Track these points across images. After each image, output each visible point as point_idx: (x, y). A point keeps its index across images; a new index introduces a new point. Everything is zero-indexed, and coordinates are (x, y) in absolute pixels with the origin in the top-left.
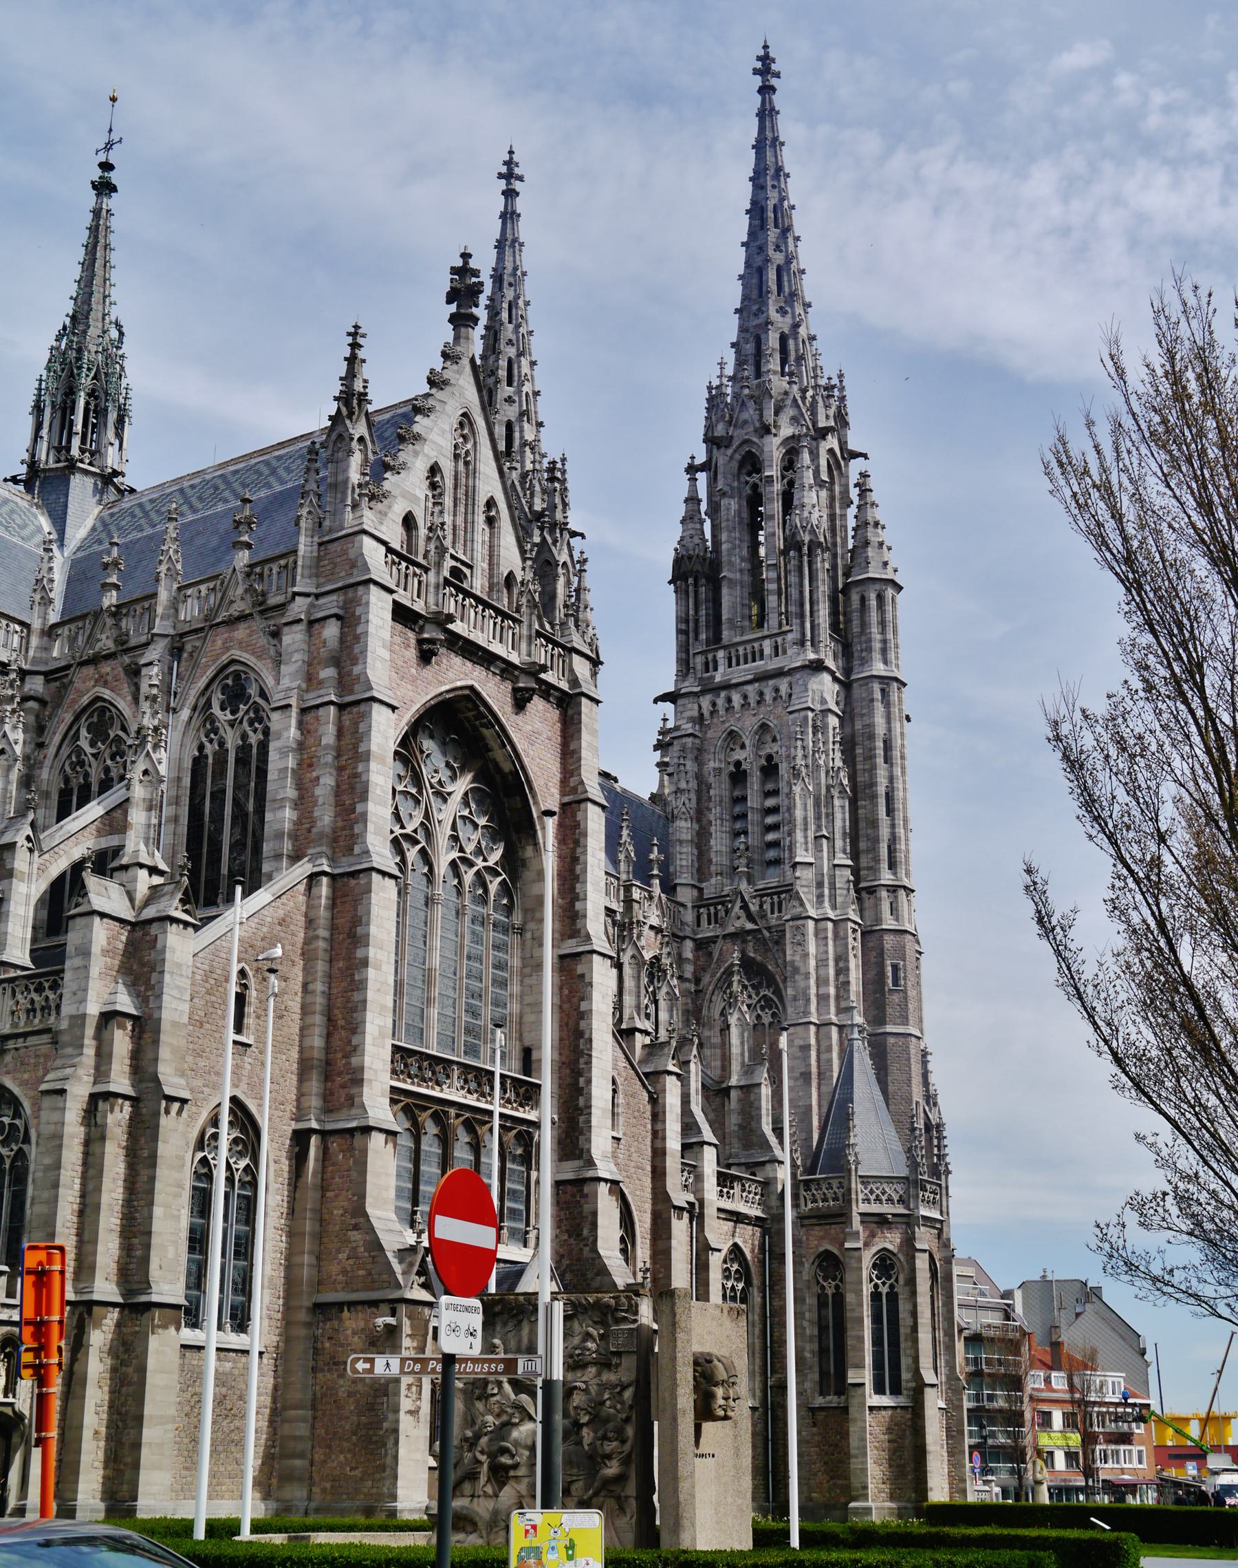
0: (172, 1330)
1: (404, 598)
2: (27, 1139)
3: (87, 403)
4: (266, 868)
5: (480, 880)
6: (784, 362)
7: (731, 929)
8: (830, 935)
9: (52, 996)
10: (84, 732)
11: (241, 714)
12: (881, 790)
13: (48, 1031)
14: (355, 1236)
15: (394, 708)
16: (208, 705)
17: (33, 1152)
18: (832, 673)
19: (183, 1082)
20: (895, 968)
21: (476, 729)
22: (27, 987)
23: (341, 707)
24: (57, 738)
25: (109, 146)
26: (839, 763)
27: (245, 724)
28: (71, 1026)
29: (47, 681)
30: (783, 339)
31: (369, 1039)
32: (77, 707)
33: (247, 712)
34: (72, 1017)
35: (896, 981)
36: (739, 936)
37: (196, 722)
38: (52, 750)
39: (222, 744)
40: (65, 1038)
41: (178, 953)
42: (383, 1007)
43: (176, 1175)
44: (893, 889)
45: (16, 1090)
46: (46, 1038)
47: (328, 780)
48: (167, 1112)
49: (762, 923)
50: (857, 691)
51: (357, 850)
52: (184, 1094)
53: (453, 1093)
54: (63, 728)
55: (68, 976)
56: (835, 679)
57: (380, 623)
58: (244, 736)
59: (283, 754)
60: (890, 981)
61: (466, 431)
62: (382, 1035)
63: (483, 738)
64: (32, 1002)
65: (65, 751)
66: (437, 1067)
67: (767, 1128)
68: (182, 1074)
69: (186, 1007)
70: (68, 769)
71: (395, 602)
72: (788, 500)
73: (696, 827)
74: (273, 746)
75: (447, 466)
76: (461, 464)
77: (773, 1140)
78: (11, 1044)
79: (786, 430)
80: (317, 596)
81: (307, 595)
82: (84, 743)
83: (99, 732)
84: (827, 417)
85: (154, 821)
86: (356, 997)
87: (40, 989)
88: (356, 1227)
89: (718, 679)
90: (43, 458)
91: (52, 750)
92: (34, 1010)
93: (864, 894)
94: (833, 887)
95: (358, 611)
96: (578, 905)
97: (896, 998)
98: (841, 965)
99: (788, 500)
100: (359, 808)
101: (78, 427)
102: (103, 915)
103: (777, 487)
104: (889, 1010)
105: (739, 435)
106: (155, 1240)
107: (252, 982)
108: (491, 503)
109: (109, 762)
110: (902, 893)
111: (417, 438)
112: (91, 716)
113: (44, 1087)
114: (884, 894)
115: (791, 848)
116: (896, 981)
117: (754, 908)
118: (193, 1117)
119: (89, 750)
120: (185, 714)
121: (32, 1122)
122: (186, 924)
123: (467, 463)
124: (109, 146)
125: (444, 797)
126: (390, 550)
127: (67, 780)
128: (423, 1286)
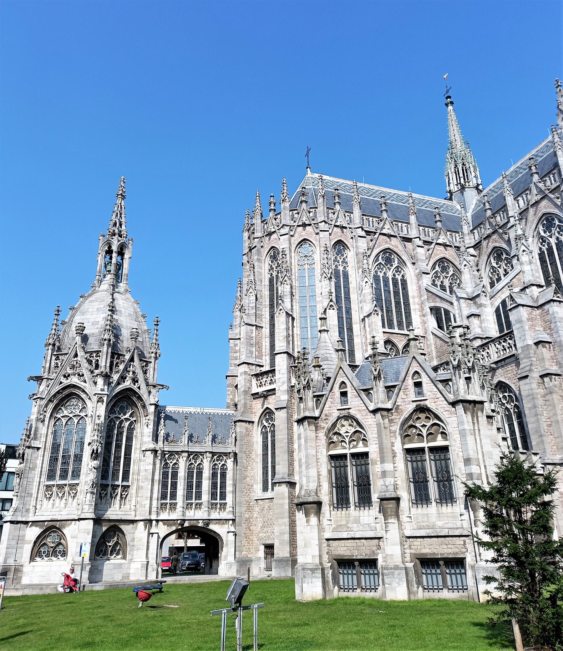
9: (510, 342)
10: (492, 261)
13: (514, 355)
22: (499, 342)
28: (522, 351)
32: (488, 253)
34: (522, 347)
38: (483, 270)
40: (521, 356)
45: (507, 382)
46: (513, 359)
54: (485, 262)
55: (515, 332)
64: (503, 346)
65: (488, 269)
70: (490, 275)
78: (499, 364)
82: (494, 265)
83: (499, 258)
87: (505, 341)
91: (483, 270)
92: (505, 350)
109: (505, 267)
112: (494, 254)
113: (519, 376)
119: (496, 266)
127: (491, 278)
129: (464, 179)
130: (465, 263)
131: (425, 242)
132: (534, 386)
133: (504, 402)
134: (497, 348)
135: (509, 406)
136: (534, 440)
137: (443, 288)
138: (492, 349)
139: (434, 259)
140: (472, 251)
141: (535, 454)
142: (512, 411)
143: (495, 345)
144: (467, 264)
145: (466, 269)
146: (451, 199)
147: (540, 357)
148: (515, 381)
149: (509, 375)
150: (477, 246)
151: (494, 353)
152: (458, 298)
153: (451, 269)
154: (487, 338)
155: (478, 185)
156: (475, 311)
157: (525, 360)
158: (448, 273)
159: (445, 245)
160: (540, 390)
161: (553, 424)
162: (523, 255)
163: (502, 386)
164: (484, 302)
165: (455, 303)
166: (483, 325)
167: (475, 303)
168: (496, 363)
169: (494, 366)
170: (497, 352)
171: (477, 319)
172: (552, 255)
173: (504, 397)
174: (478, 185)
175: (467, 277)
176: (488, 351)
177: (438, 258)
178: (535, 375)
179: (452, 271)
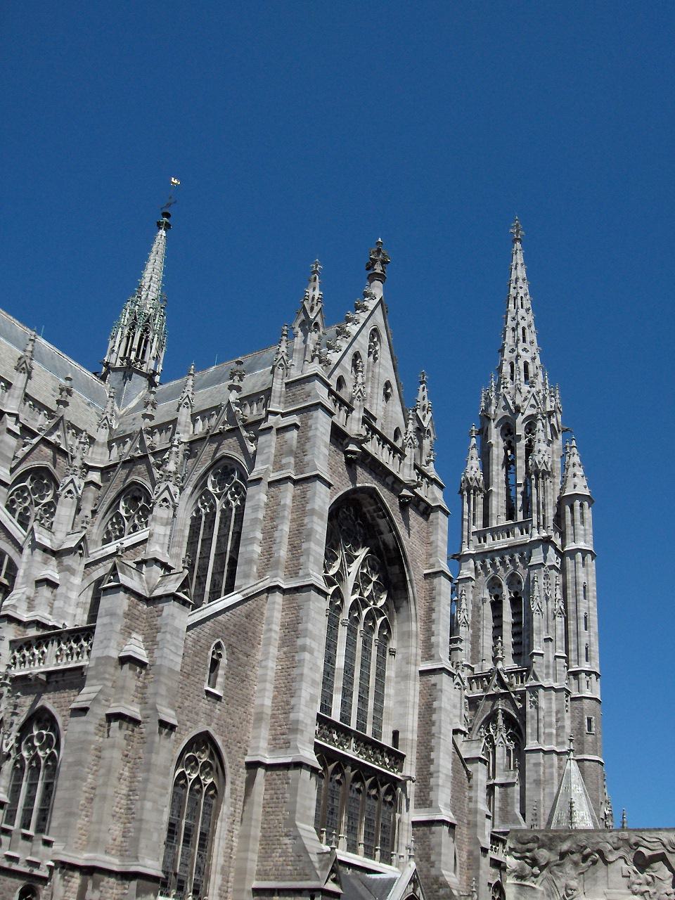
0: (152, 896)
1: (340, 419)
2: (58, 747)
3: (142, 335)
4: (237, 583)
5: (370, 616)
6: (526, 377)
7: (491, 692)
8: (554, 698)
9: (85, 644)
11: (226, 489)
12: (582, 615)
13: (81, 668)
14: (286, 840)
15: (329, 485)
16: (205, 484)
17: (62, 755)
18: (554, 545)
19: (173, 713)
20: (589, 720)
21: (373, 519)
23: (296, 482)
24: (105, 507)
25: (169, 205)
26: (559, 596)
27: (229, 496)
28: (97, 665)
29: (102, 475)
30: (526, 364)
31: (303, 701)
33: (230, 489)
34: (98, 658)
35: (590, 729)
36: (494, 698)
37: (196, 495)
39: (213, 507)
40: (89, 674)
41: (177, 621)
42: (314, 682)
43: (161, 779)
44: (588, 673)
47: (286, 528)
48: (160, 733)
49: (511, 689)
50: (568, 559)
51: (301, 573)
52: (174, 722)
53: (350, 752)
55: (97, 630)
56: (557, 550)
57: (324, 431)
58: (228, 503)
59: (256, 509)
60: (586, 728)
61: (375, 340)
62: (313, 699)
63: (378, 525)
65: (109, 516)
66: (345, 732)
67: (517, 811)
68: (172, 706)
69: (179, 660)
70: (110, 528)
71: (333, 423)
72: (529, 449)
73: (471, 631)
74: (247, 504)
75: (364, 354)
76: (372, 357)
77: (521, 818)
79: (529, 412)
80: (283, 415)
81: (275, 414)
84: (551, 406)
85: (168, 533)
86: (295, 672)
87: (77, 641)
88: (286, 835)
89: (486, 547)
90: (114, 362)
93: (571, 677)
94: (555, 668)
95: (310, 422)
96: (433, 639)
97: (590, 738)
98: (559, 715)
99: (529, 449)
100: (304, 546)
101: (135, 346)
102: (127, 590)
103: (524, 442)
104: (586, 746)
105: (501, 413)
106: (145, 826)
107: (224, 653)
108: (388, 385)
109: (136, 522)
110: (593, 675)
111: (348, 335)
113: (74, 705)
114: (583, 675)
115: (530, 646)
116: (590, 729)
117: (506, 680)
118: (177, 741)
119: (123, 513)
120: (189, 490)
121: (63, 733)
122: (184, 603)
123: (375, 359)
124: (169, 205)
125: (351, 559)
126: (331, 392)
128: (334, 881)
129: (137, 355)
130: (71, 487)
131: (25, 429)
132: (92, 728)
133: (37, 744)
134: (61, 650)
135: (41, 754)
136: (56, 819)
137: (23, 522)
138: (52, 650)
139: (29, 464)
140: (95, 477)
141: (48, 843)
142: (43, 762)
143: (59, 644)
144: (73, 490)
145: (69, 499)
146: (103, 378)
147: (120, 683)
148: (65, 713)
149: (62, 700)
150: (105, 471)
151: (52, 659)
152: (35, 545)
153: (51, 492)
154: (55, 627)
155: (155, 373)
156: (55, 576)
157: (94, 682)
158: (42, 497)
159: (56, 448)
160: (97, 738)
161: (97, 799)
162: (161, 506)
163: (41, 717)
164: (75, 566)
165: (27, 551)
166: (57, 604)
167: (60, 563)
168: (49, 674)
169: (43, 677)
170: (57, 656)
171: (51, 589)
172: (210, 528)
173: (40, 737)
174: (155, 373)
175: (65, 510)
176: (45, 650)
177: (35, 464)
178: (100, 712)
179: (51, 496)
